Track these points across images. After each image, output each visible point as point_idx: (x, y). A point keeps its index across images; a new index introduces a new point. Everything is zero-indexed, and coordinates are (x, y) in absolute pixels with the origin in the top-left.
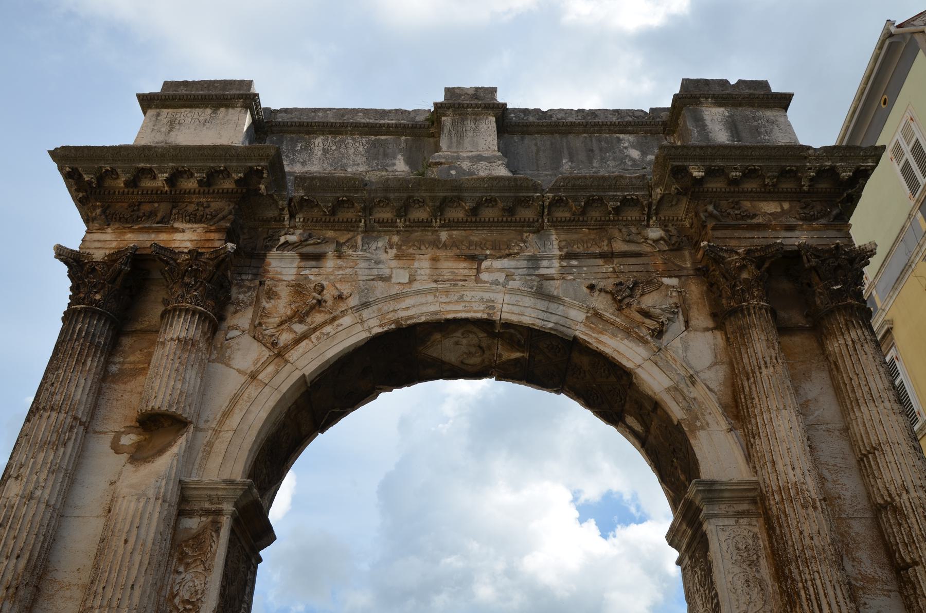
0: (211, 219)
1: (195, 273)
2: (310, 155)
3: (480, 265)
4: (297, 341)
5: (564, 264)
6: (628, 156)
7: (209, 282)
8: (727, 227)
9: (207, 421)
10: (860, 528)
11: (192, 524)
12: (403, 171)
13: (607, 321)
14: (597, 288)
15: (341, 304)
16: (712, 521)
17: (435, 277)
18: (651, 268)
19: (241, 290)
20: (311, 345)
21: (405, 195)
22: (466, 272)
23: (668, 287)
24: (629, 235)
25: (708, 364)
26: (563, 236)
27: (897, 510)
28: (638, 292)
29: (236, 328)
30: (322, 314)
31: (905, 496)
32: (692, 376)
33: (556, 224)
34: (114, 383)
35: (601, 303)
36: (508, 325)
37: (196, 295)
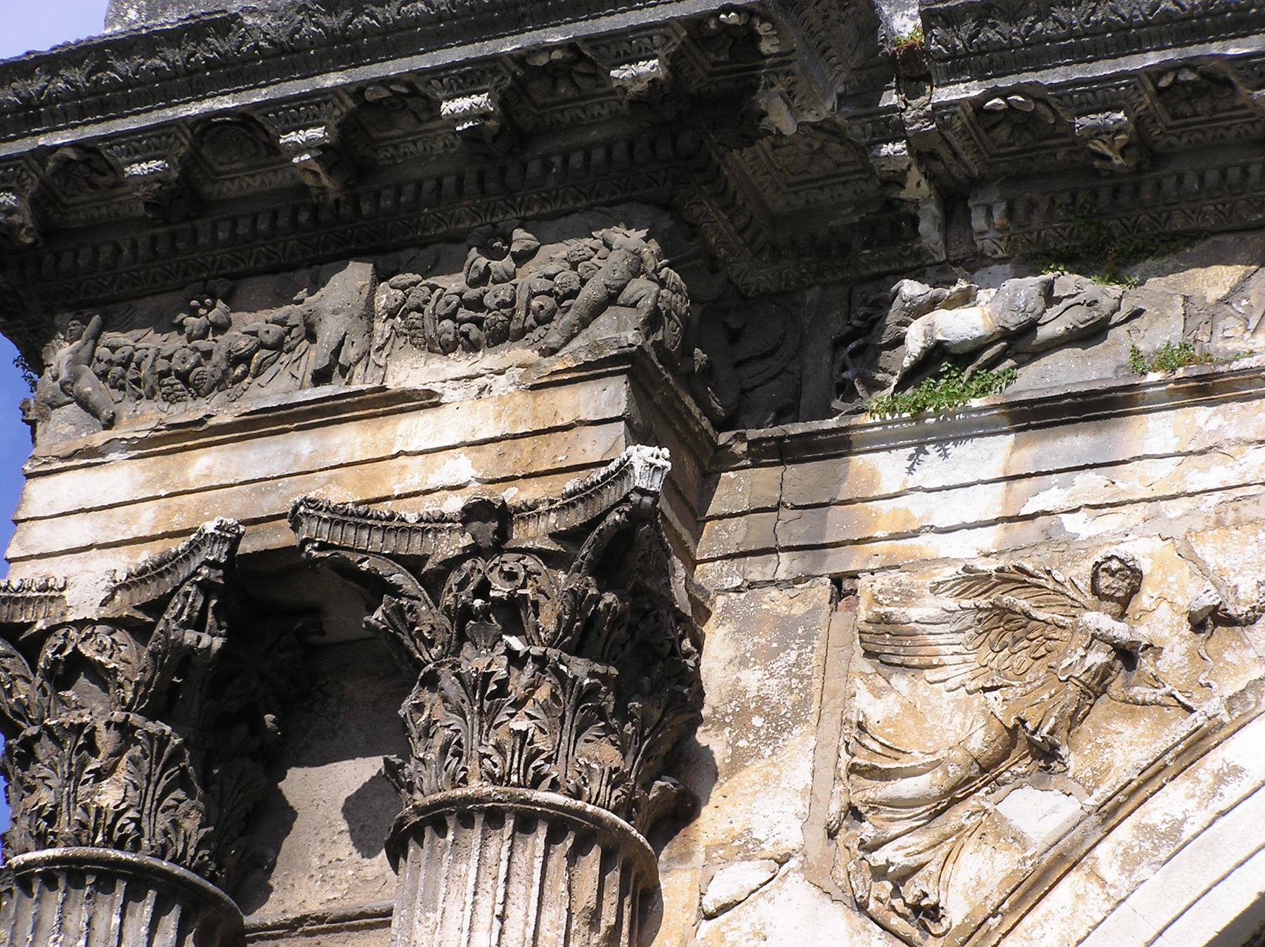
0: (544, 319)
7: (577, 650)
15: (1229, 656)
30: (1145, 723)
37: (523, 735)
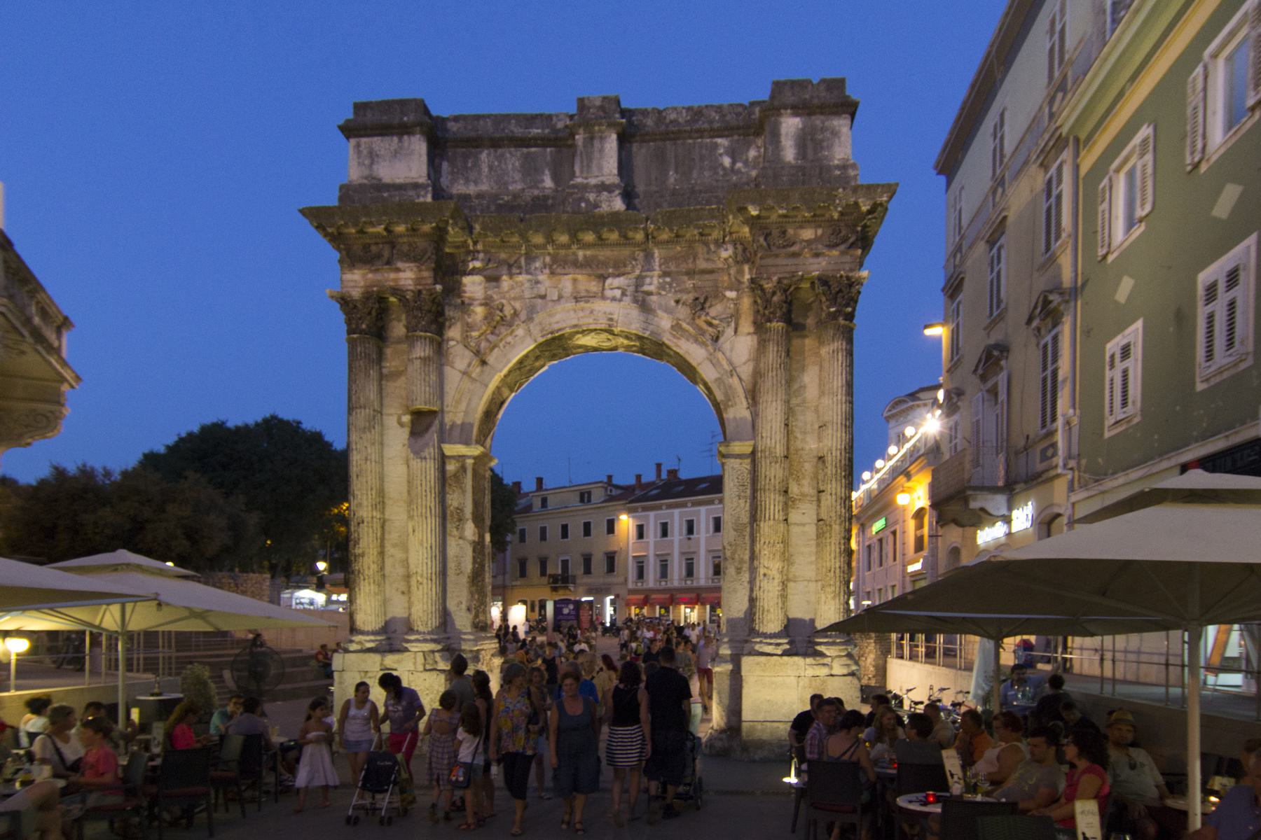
2: (480, 172)
3: (604, 282)
4: (492, 349)
5: (661, 281)
6: (722, 165)
23: (729, 299)
26: (664, 252)
27: (824, 462)
28: (707, 305)
33: (658, 244)
35: (683, 312)
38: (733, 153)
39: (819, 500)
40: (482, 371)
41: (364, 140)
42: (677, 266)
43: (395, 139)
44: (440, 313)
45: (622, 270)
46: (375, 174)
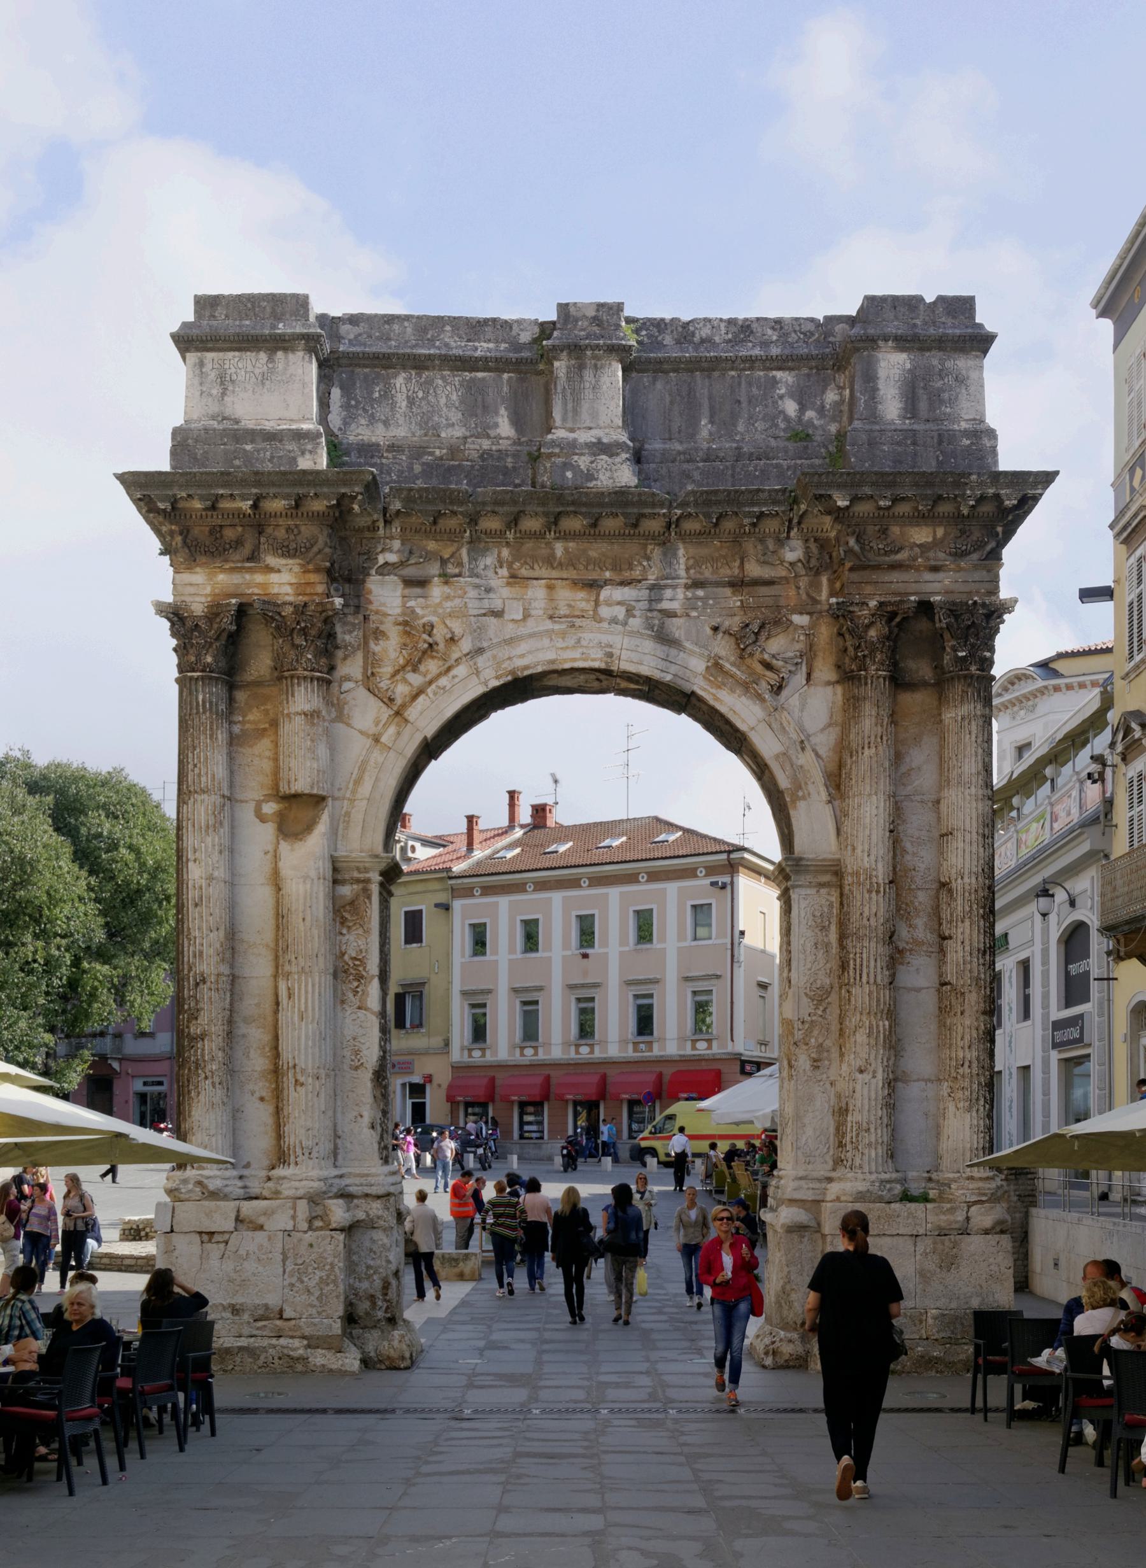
1: (304, 632)
2: (393, 406)
3: (598, 595)
4: (415, 697)
5: (689, 594)
6: (783, 412)
8: (864, 568)
9: (339, 789)
10: (923, 899)
11: (346, 891)
12: (508, 438)
13: (727, 673)
14: (722, 629)
16: (797, 890)
17: (550, 612)
18: (782, 602)
19: (346, 628)
20: (428, 702)
21: (516, 509)
22: (583, 605)
24: (764, 554)
25: (821, 726)
26: (692, 551)
27: (950, 891)
28: (763, 637)
29: (348, 679)
31: (959, 881)
32: (802, 742)
34: (241, 746)
35: (723, 648)
36: (624, 672)
38: (803, 399)
39: (942, 951)
40: (399, 733)
41: (210, 355)
42: (715, 572)
43: (263, 356)
44: (331, 636)
45: (627, 575)
46: (228, 412)
